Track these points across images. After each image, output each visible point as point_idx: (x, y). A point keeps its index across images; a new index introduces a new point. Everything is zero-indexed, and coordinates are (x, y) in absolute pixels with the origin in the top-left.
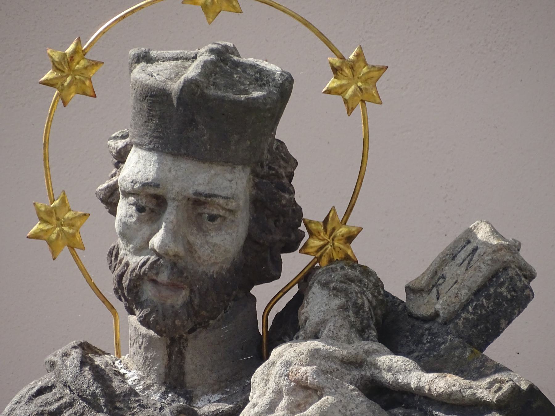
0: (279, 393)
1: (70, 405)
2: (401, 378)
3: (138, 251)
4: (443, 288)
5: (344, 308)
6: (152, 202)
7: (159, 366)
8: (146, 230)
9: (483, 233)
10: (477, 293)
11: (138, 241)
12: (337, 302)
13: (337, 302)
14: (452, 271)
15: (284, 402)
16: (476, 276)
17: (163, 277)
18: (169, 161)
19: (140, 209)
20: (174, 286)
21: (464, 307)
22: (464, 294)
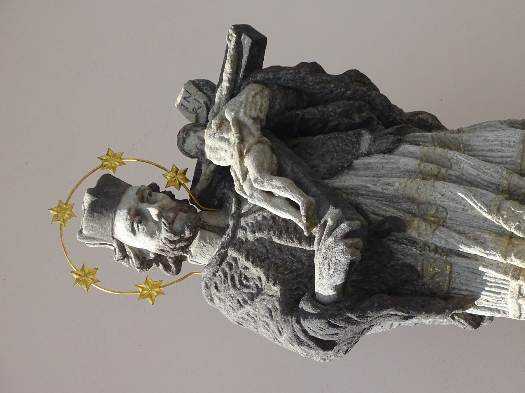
0: (222, 139)
1: (223, 269)
2: (224, 92)
3: (160, 229)
4: (197, 105)
5: (195, 132)
6: (138, 217)
7: (214, 236)
8: (151, 224)
9: (179, 99)
10: (201, 90)
11: (155, 228)
12: (192, 134)
13: (192, 134)
14: (191, 106)
15: (225, 136)
16: (193, 90)
17: (171, 215)
18: (121, 205)
19: (140, 222)
20: (176, 214)
21: (204, 93)
22: (199, 93)
